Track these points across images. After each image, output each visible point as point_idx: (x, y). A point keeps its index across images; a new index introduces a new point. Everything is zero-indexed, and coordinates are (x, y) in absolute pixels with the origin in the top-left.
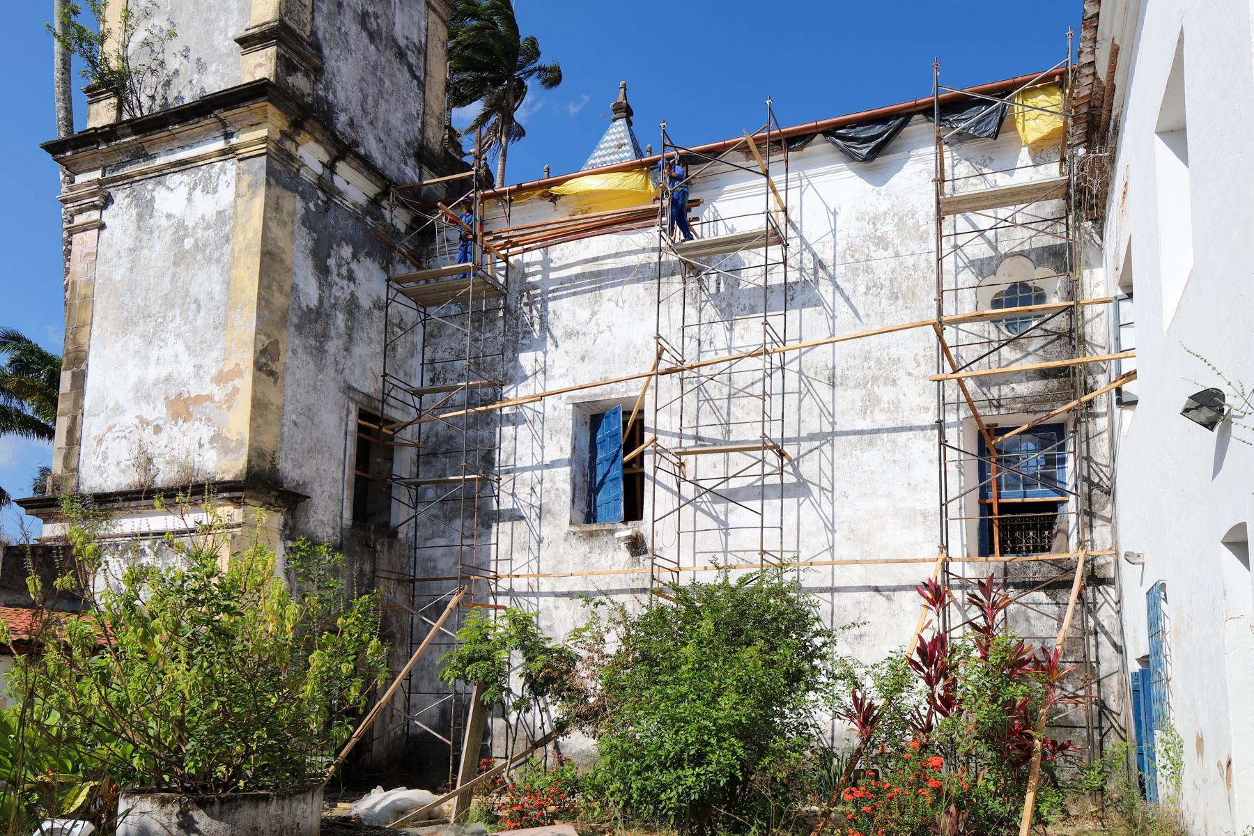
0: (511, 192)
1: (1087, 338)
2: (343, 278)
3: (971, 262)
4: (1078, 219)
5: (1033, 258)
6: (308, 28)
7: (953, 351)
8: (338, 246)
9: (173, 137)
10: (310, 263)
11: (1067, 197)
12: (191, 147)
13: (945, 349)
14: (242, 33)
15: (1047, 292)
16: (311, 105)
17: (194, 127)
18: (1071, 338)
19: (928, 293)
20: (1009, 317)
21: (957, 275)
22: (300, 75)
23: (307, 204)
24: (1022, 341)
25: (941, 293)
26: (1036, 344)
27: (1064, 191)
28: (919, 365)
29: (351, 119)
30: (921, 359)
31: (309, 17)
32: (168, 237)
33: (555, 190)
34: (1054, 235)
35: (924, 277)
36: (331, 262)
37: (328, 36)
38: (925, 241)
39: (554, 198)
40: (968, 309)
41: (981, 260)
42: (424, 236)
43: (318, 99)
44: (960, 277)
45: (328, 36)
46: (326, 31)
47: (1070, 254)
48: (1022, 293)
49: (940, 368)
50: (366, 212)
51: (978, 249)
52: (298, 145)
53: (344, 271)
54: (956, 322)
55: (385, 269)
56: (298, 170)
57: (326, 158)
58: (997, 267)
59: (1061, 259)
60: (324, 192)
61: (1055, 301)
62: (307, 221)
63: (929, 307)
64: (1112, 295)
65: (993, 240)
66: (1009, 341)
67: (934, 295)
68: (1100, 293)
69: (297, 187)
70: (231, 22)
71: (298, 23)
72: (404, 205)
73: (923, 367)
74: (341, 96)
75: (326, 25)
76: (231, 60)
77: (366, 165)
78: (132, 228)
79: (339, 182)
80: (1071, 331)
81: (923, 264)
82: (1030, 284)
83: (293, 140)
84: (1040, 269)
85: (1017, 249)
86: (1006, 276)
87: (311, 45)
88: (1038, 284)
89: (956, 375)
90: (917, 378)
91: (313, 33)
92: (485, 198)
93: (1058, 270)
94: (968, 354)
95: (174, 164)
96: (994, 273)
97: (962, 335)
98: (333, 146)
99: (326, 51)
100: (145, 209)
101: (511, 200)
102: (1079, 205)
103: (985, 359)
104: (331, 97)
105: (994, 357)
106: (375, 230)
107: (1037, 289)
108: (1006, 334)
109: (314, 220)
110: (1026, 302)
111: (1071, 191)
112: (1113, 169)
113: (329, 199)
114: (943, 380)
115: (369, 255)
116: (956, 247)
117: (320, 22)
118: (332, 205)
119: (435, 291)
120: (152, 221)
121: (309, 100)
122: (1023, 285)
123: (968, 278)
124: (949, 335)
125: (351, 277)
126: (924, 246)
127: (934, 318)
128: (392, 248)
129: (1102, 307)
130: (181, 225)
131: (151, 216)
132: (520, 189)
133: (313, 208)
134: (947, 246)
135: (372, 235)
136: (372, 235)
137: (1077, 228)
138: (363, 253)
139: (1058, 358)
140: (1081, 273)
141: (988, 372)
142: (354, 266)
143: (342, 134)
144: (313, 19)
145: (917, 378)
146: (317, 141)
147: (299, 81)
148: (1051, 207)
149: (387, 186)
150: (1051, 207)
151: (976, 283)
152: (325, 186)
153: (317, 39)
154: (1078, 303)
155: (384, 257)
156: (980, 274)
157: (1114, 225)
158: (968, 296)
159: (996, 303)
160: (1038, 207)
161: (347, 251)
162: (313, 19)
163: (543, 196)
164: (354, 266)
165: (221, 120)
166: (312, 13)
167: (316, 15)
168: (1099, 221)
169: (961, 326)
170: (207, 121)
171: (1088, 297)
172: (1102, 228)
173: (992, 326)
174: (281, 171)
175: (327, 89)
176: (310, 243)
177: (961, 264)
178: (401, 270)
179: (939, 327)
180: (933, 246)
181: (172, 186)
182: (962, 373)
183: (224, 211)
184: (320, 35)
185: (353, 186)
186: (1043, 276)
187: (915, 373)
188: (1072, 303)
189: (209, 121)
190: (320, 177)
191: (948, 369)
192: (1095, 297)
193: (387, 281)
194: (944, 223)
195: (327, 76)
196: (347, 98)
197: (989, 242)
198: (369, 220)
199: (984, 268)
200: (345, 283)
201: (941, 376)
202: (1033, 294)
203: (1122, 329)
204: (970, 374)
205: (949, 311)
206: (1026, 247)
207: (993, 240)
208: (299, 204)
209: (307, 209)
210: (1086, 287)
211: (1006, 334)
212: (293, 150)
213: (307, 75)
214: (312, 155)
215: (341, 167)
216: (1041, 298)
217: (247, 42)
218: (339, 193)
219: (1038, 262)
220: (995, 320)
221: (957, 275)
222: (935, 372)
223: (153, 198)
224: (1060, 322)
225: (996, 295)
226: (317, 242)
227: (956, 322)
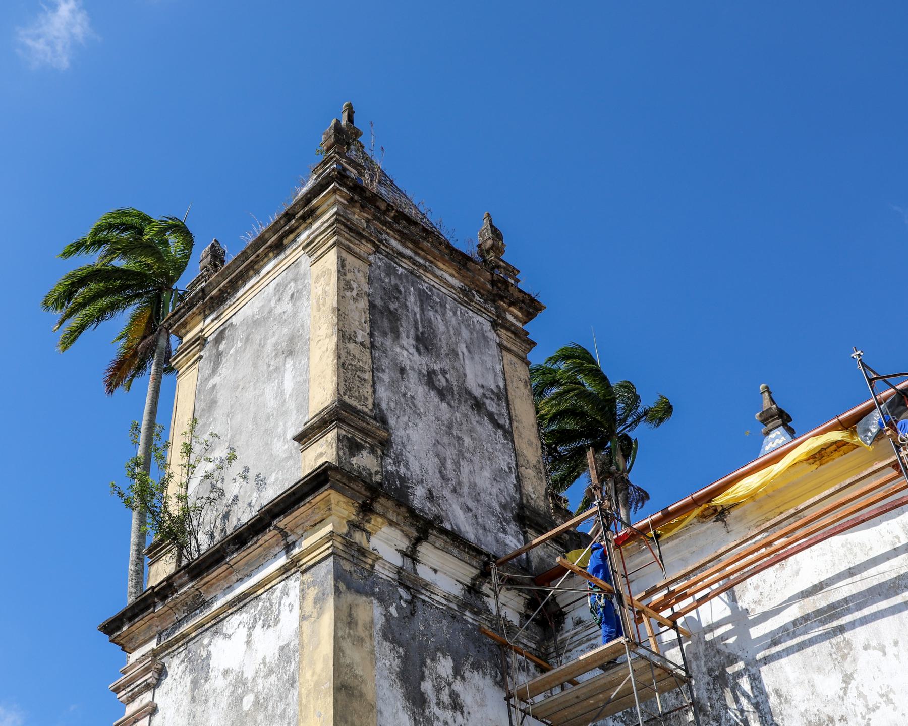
0: (655, 523)
2: (444, 708)
6: (370, 402)
8: (433, 660)
9: (231, 570)
10: (399, 692)
12: (249, 576)
14: (301, 429)
16: (381, 484)
17: (253, 549)
22: (365, 453)
23: (386, 608)
29: (429, 490)
31: (370, 390)
32: (224, 702)
33: (720, 500)
36: (427, 686)
37: (392, 405)
39: (721, 514)
42: (547, 618)
43: (388, 476)
45: (392, 405)
46: (390, 400)
50: (464, 605)
52: (369, 534)
53: (445, 697)
55: (501, 684)
56: (372, 566)
57: (404, 544)
60: (407, 588)
62: (390, 634)
69: (372, 589)
70: (289, 424)
71: (358, 399)
72: (511, 583)
74: (415, 466)
75: (390, 394)
76: (290, 463)
77: (456, 540)
78: (186, 700)
79: (424, 572)
83: (364, 530)
87: (375, 419)
91: (376, 405)
92: (620, 543)
95: (231, 604)
98: (412, 525)
99: (392, 422)
100: (200, 670)
101: (658, 537)
104: (402, 470)
106: (479, 629)
109: (401, 632)
113: (414, 597)
115: (476, 666)
117: (383, 393)
118: (419, 604)
119: (579, 700)
120: (207, 686)
121: (378, 478)
125: (456, 705)
128: (503, 648)
130: (240, 680)
131: (207, 679)
132: (668, 515)
133: (395, 613)
135: (476, 636)
136: (476, 636)
138: (468, 666)
142: (458, 686)
143: (421, 510)
144: (374, 392)
146: (391, 523)
147: (365, 461)
149: (485, 563)
152: (409, 582)
153: (381, 410)
155: (496, 666)
161: (445, 666)
162: (374, 392)
163: (703, 517)
164: (458, 686)
165: (281, 531)
166: (373, 386)
167: (378, 386)
170: (266, 537)
174: (353, 571)
175: (397, 462)
176: (396, 663)
178: (522, 680)
181: (229, 632)
183: (287, 645)
184: (384, 406)
185: (444, 574)
189: (270, 535)
190: (400, 570)
193: (507, 699)
195: (396, 447)
196: (422, 467)
198: (468, 616)
200: (448, 715)
208: (377, 611)
209: (388, 616)
212: (364, 543)
213: (373, 451)
214: (386, 542)
215: (426, 551)
217: (304, 438)
218: (426, 586)
223: (209, 654)
226: (405, 660)
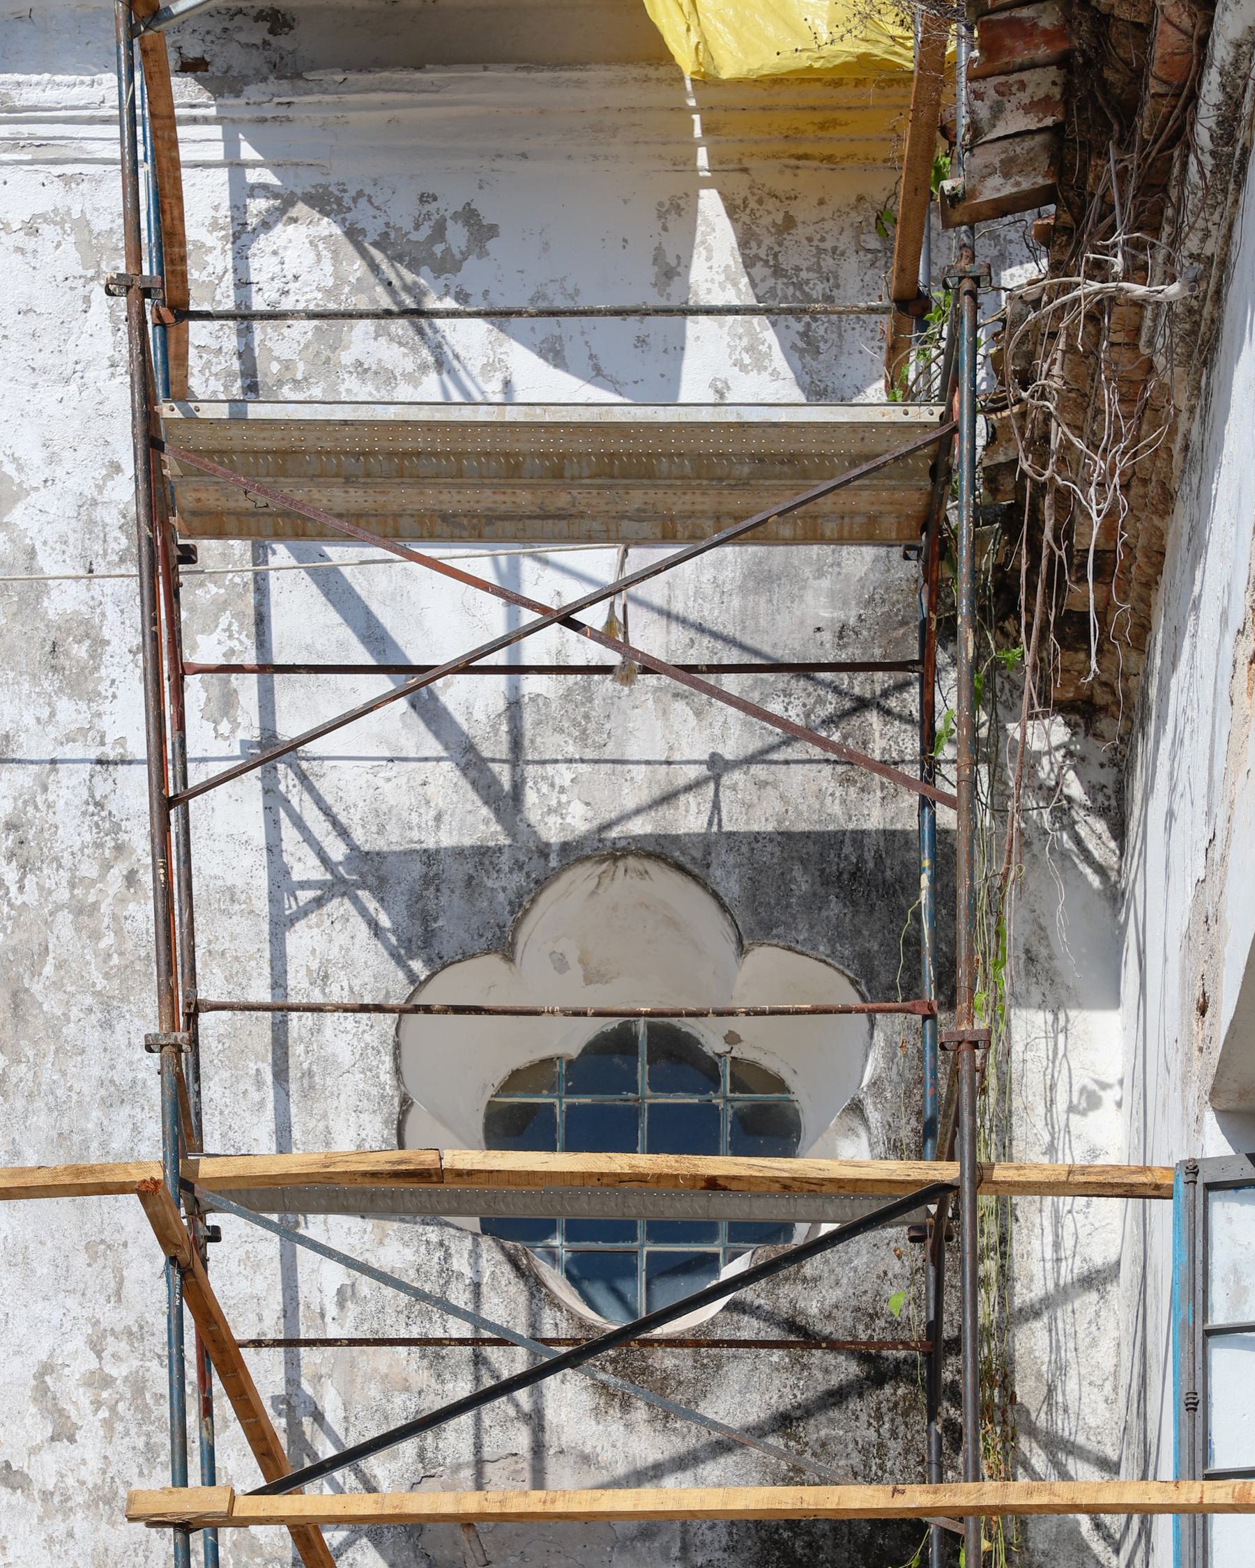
1: (1027, 1391)
3: (359, 856)
4: (988, 689)
5: (732, 888)
7: (266, 1372)
11: (932, 545)
13: (221, 1352)
15: (804, 1096)
18: (937, 1393)
19: (108, 1011)
20: (588, 1208)
21: (280, 925)
24: (666, 1360)
25: (185, 1010)
26: (745, 1393)
27: (912, 497)
28: (64, 1432)
30: (76, 1402)
34: (850, 760)
35: (83, 910)
38: (80, 684)
40: (347, 1128)
41: (430, 857)
44: (300, 940)
47: (944, 896)
48: (646, 1076)
49: (185, 1455)
51: (392, 783)
54: (283, 1199)
58: (520, 906)
59: (896, 920)
61: (850, 1153)
63: (118, 1096)
64: (1168, 1153)
65: (494, 746)
66: (580, 1353)
67: (144, 1014)
68: (1106, 1139)
73: (90, 1445)
80: (937, 1346)
81: (71, 832)
82: (711, 1037)
84: (765, 957)
85: (639, 827)
86: (574, 973)
88: (762, 1044)
89: (286, 1504)
90: (55, 1502)
93: (865, 974)
94: (350, 1395)
96: (504, 947)
97: (321, 1279)
102: (999, 603)
103: (455, 1438)
105: (504, 1430)
107: (750, 1076)
108: (573, 1310)
110: (687, 1132)
111: (958, 515)
112: (1206, 399)
114: (212, 1524)
116: (271, 753)
122: (675, 1051)
123: (344, 950)
124: (242, 1266)
126: (69, 712)
127: (142, 1145)
129: (1103, 1228)
134: (211, 741)
137: (983, 751)
139: (862, 1475)
140: (1000, 1017)
141: (471, 1503)
145: (55, 1502)
148: (830, 591)
150: (830, 591)
151: (399, 991)
154: (979, 1177)
156: (420, 941)
157: (1195, 753)
158: (346, 1052)
159: (511, 1124)
160: (760, 580)
168: (1110, 716)
169: (316, 1226)
171: (1030, 1151)
172: (1122, 764)
173: (491, 1257)
177: (305, 867)
179: (182, 1208)
180: (127, 722)
182: (315, 1499)
186: (771, 999)
187: (46, 1469)
188: (947, 1171)
191: (239, 1465)
192: (1074, 1155)
194: (197, 594)
197: (470, 760)
199: (448, 909)
201: (197, 1499)
202: (726, 1100)
203: (1223, 1358)
204: (365, 1505)
205: (239, 1131)
206: (690, 818)
207: (494, 746)
210: (1029, 1097)
211: (573, 1310)
216: (772, 1127)
219: (757, 921)
220: (513, 1223)
221: (280, 925)
222: (164, 1477)
224: (867, 1278)
225: (516, 1080)
227: (283, 1199)
